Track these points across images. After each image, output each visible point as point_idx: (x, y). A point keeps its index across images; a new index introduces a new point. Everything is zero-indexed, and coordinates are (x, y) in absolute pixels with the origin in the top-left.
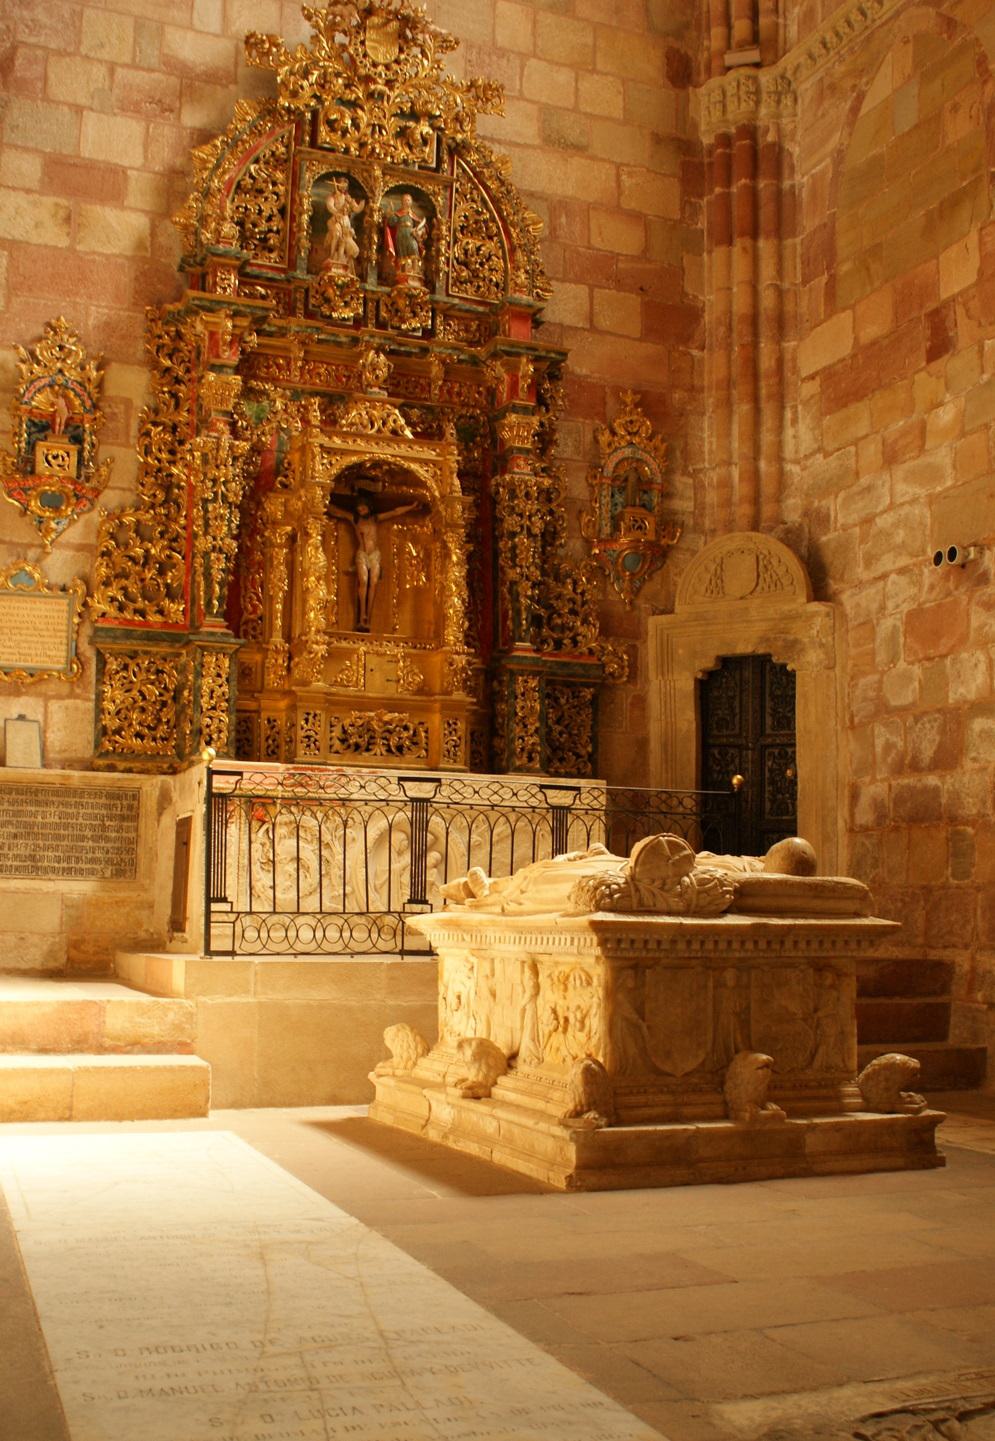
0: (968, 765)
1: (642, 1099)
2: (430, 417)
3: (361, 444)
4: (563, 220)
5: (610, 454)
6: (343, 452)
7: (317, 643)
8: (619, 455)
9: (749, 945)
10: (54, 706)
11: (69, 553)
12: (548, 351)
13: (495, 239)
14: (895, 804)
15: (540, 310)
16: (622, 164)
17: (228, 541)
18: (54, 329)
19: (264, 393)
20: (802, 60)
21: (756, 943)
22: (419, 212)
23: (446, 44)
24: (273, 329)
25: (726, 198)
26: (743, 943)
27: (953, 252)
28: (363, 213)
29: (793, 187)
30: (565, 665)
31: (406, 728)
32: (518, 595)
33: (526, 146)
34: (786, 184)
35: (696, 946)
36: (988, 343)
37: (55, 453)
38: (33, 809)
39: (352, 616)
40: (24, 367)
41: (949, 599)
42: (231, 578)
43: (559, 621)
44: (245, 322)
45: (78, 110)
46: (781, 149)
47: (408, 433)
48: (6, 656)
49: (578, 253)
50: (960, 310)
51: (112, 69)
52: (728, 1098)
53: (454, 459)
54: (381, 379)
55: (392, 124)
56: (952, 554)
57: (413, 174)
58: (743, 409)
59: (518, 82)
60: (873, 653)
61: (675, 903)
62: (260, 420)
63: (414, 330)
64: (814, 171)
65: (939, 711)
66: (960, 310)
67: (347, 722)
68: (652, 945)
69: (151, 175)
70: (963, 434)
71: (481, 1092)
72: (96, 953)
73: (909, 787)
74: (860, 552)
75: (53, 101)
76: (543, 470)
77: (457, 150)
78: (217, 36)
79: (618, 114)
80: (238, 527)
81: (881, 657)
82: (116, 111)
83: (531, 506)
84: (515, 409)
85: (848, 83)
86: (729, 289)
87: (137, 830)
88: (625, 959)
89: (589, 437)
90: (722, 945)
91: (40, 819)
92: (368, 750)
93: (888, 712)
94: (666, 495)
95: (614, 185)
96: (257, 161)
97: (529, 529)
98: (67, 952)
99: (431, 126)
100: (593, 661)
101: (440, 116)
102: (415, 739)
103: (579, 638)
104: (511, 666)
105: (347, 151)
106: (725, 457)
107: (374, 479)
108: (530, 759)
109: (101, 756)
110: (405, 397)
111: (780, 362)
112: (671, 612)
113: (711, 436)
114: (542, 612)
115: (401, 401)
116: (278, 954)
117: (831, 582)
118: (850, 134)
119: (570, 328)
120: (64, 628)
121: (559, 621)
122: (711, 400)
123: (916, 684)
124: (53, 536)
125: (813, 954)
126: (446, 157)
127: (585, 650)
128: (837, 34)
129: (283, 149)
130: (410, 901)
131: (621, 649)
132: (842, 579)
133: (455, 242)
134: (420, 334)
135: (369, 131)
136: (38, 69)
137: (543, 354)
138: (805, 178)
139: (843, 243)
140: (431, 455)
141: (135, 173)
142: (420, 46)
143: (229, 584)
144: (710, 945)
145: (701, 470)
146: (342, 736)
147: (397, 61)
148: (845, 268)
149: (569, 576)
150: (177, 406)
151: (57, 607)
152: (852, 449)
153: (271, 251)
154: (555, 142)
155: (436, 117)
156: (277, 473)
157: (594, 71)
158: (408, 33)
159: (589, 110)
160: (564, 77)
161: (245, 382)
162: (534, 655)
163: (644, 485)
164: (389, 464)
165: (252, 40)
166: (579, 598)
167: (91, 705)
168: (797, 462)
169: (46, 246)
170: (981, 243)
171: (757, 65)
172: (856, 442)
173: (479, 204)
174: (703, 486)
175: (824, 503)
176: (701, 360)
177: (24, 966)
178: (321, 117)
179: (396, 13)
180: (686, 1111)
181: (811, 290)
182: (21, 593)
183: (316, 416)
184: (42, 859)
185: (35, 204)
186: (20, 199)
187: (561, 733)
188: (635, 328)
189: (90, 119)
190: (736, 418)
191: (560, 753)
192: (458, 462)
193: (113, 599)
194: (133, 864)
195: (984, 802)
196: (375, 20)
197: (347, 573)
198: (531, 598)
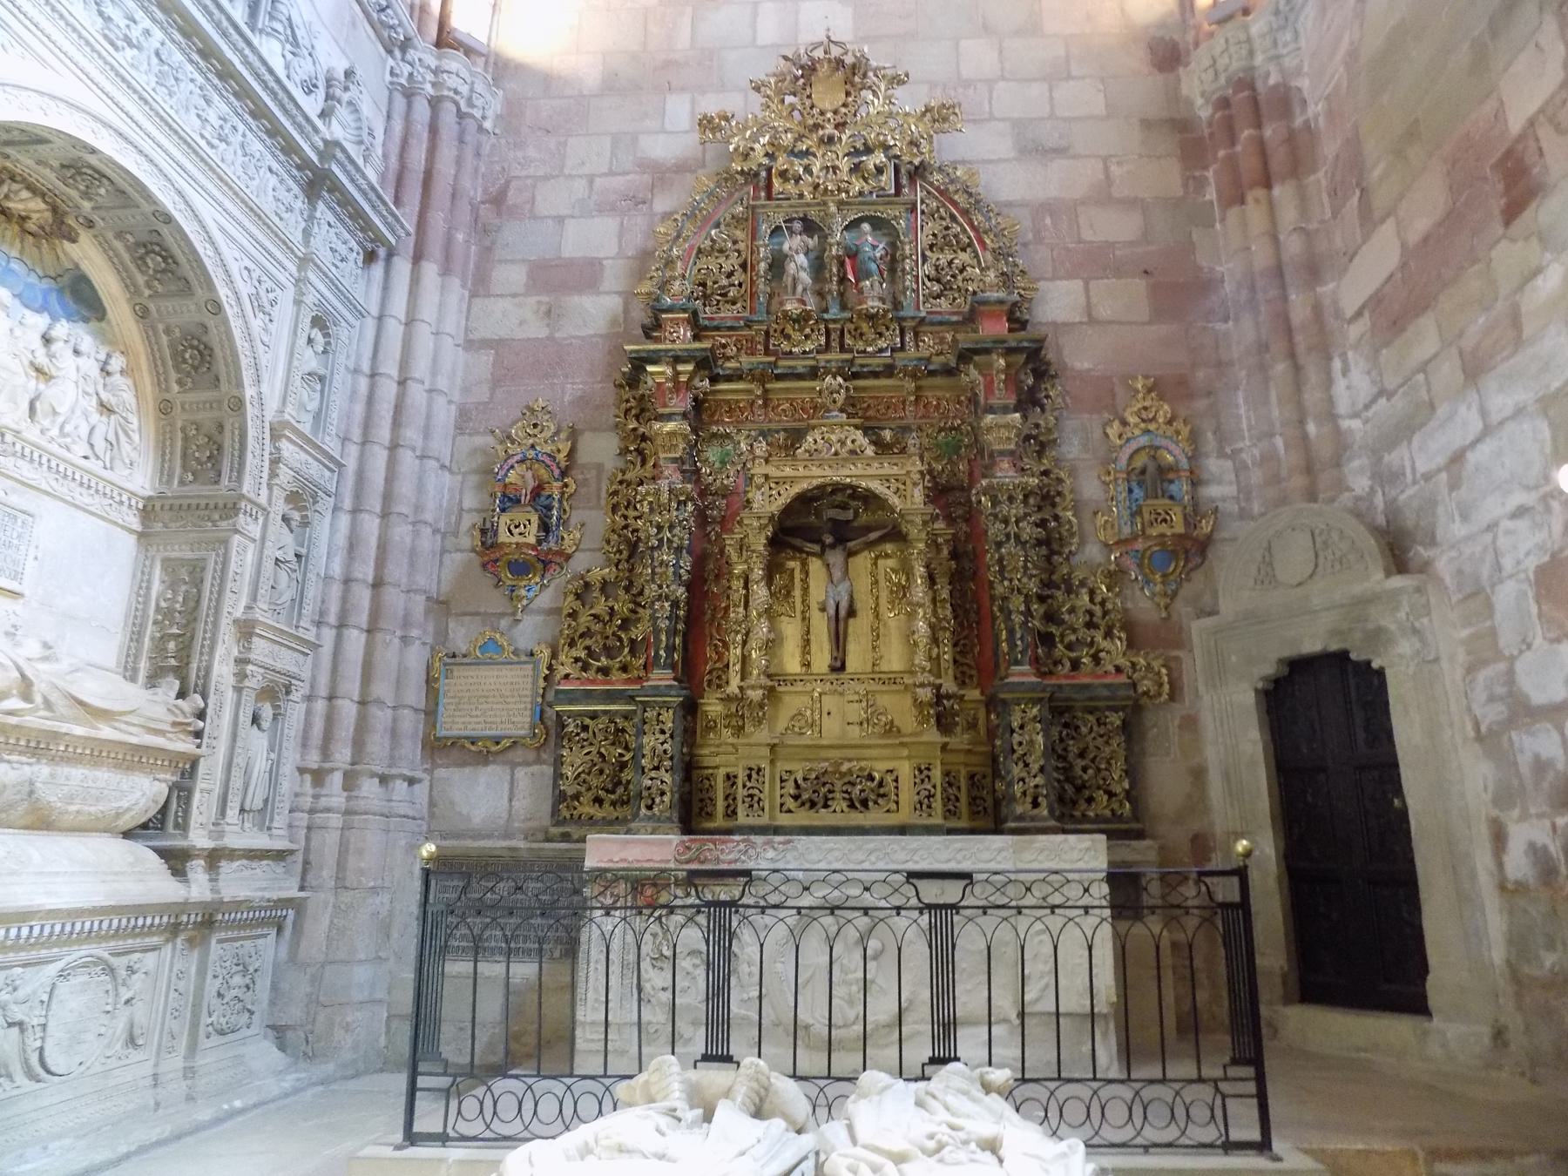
5: (1121, 447)
6: (792, 480)
8: (1134, 445)
10: (521, 773)
11: (539, 618)
13: (968, 250)
18: (532, 411)
19: (728, 436)
23: (897, 81)
25: (1231, 161)
31: (871, 778)
33: (1000, 161)
40: (499, 447)
45: (560, 220)
51: (591, 179)
54: (839, 404)
55: (845, 164)
60: (1493, 633)
63: (881, 350)
75: (541, 218)
77: (919, 172)
78: (686, 132)
82: (594, 213)
83: (1016, 510)
84: (991, 410)
89: (1098, 433)
94: (1196, 483)
95: (1102, 177)
96: (717, 225)
97: (1017, 537)
102: (882, 791)
104: (1002, 696)
105: (801, 196)
108: (1035, 804)
111: (1317, 310)
113: (1249, 410)
119: (1065, 324)
120: (529, 693)
122: (1243, 373)
124: (525, 602)
126: (904, 181)
127: (1111, 668)
131: (1156, 664)
132: (1432, 542)
140: (888, 469)
141: (610, 261)
142: (870, 88)
145: (1241, 450)
146: (796, 792)
150: (644, 463)
151: (522, 673)
152: (1421, 377)
153: (734, 303)
154: (1033, 150)
155: (891, 147)
157: (1069, 77)
159: (1067, 114)
163: (1164, 473)
166: (1097, 610)
172: (1423, 368)
173: (948, 220)
182: (492, 663)
186: (506, 304)
189: (571, 227)
193: (577, 660)
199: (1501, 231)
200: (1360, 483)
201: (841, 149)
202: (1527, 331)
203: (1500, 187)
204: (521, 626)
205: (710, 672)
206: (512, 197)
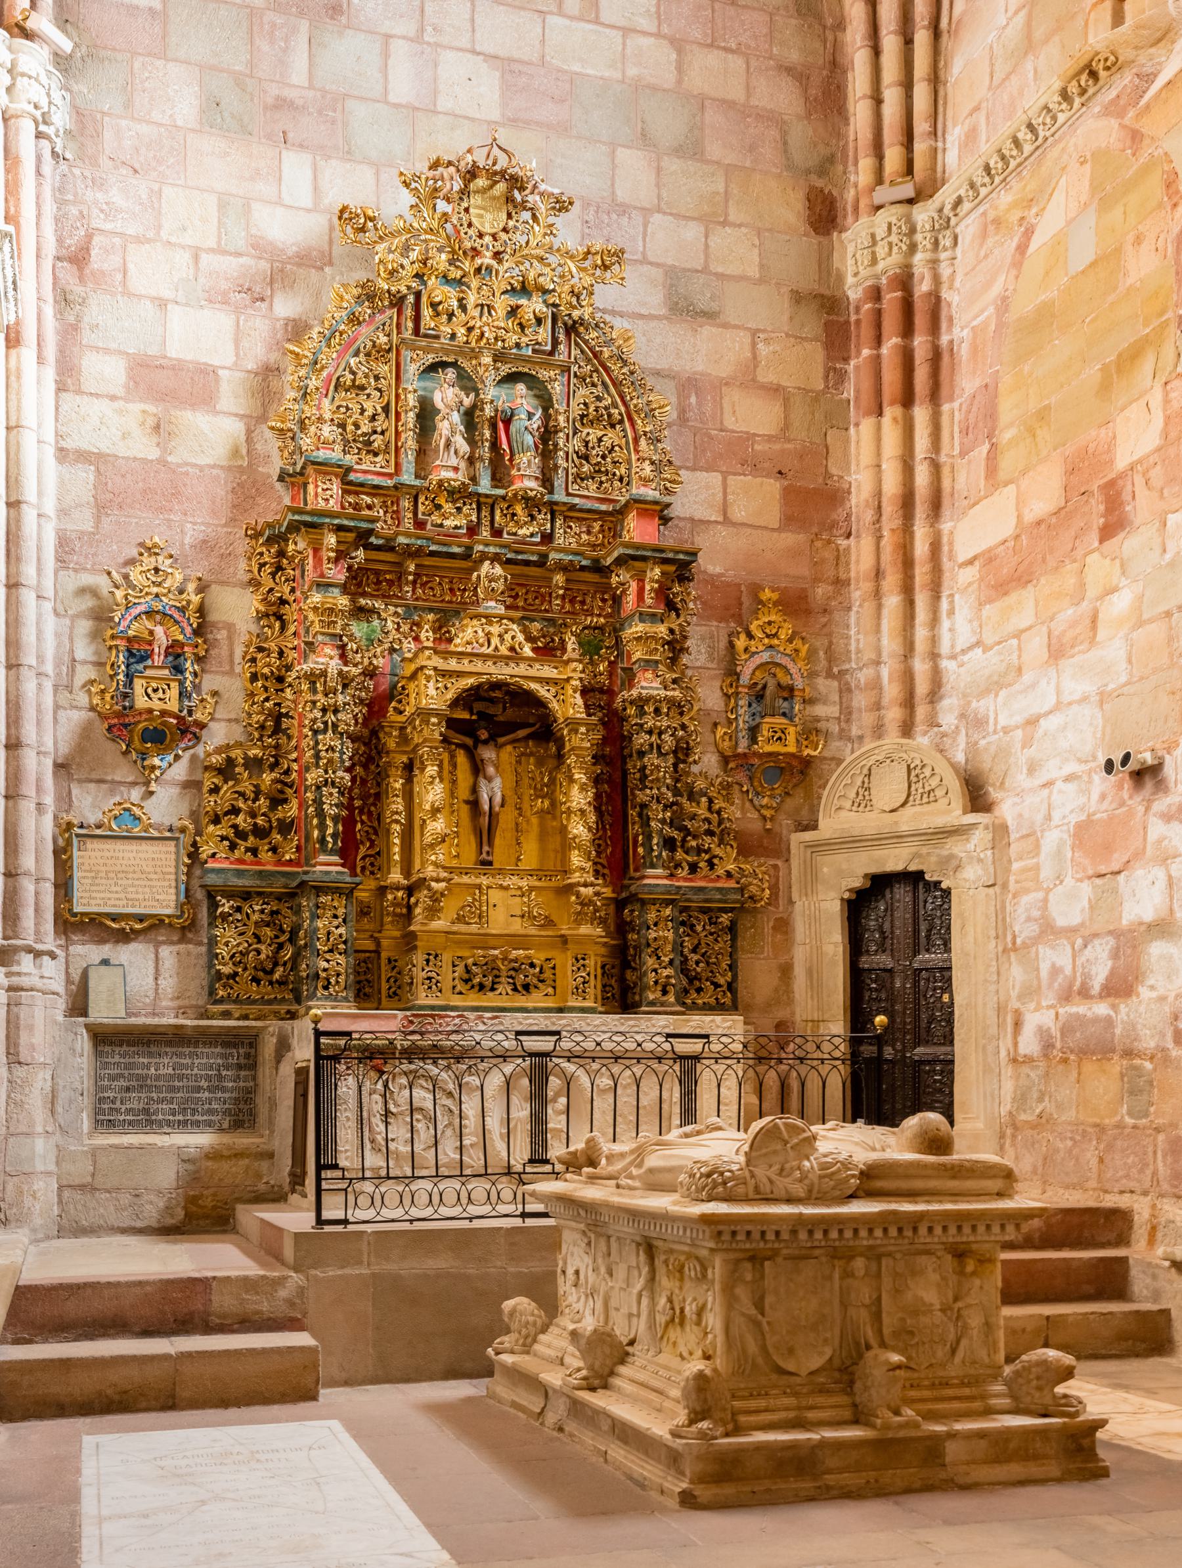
0: (1144, 992)
1: (762, 1403)
2: (552, 630)
3: (479, 666)
4: (693, 399)
7: (438, 880)
9: (878, 1233)
12: (678, 552)
14: (1062, 1034)
15: (668, 505)
16: (759, 330)
17: (340, 773)
19: (372, 611)
20: (962, 192)
21: (885, 1230)
22: (535, 402)
23: (561, 205)
24: (381, 542)
26: (871, 1231)
27: (1135, 411)
28: (474, 407)
29: (951, 342)
30: (701, 889)
32: (649, 819)
34: (944, 339)
35: (818, 1235)
36: (1172, 519)
37: (154, 685)
38: (146, 1061)
39: (474, 845)
41: (1125, 809)
42: (344, 813)
43: (694, 843)
44: (351, 536)
45: (162, 304)
46: (938, 299)
47: (527, 651)
48: (112, 902)
49: (711, 438)
50: (1139, 480)
52: (858, 1400)
53: (575, 672)
55: (502, 304)
56: (1126, 758)
57: (526, 360)
58: (893, 601)
59: (641, 243)
60: (1037, 868)
61: (799, 1190)
62: (371, 641)
64: (975, 323)
65: (1110, 933)
66: (1139, 480)
67: (470, 961)
68: (770, 1236)
69: (242, 375)
70: (1140, 624)
71: (596, 1382)
72: (214, 1207)
73: (1077, 1017)
74: (1021, 757)
76: (674, 681)
78: (308, 211)
79: (754, 272)
80: (351, 758)
81: (1046, 873)
85: (1014, 217)
86: (879, 466)
87: (254, 1078)
88: (741, 1250)
90: (848, 1234)
91: (153, 1070)
92: (493, 989)
93: (1053, 933)
96: (357, 354)
97: (659, 747)
98: (185, 1208)
99: (545, 302)
100: (732, 884)
101: (554, 290)
103: (716, 861)
105: (453, 336)
106: (873, 656)
107: (492, 701)
109: (216, 1002)
110: (524, 609)
112: (815, 827)
114: (676, 834)
115: (519, 614)
116: (393, 1221)
117: (991, 789)
118: (1017, 277)
121: (694, 843)
123: (1085, 903)
124: (158, 773)
125: (951, 1240)
126: (562, 337)
128: (1003, 158)
129: (385, 339)
130: (531, 1161)
133: (575, 434)
134: (538, 539)
135: (476, 313)
136: (115, 260)
137: (671, 555)
138: (966, 332)
139: (1007, 410)
141: (226, 372)
143: (344, 819)
144: (834, 1234)
147: (505, 230)
148: (1007, 435)
149: (705, 795)
150: (283, 628)
151: (164, 849)
152: (1015, 642)
153: (376, 454)
156: (391, 697)
158: (518, 196)
160: (692, 232)
161: (353, 601)
162: (666, 882)
164: (508, 684)
165: (346, 215)
167: (204, 949)
168: (953, 657)
169: (135, 459)
170: (1166, 401)
171: (911, 202)
172: (1018, 635)
174: (849, 690)
175: (982, 702)
176: (848, 549)
177: (139, 1224)
178: (424, 299)
179: (503, 173)
180: (811, 1415)
181: (970, 462)
183: (427, 635)
184: (156, 1112)
185: (120, 412)
187: (697, 963)
188: (773, 516)
190: (885, 612)
191: (697, 983)
192: (581, 679)
193: (223, 838)
194: (252, 1115)
195: (1163, 1035)
196: (481, 182)
197: (467, 802)
198: (663, 821)
199: (1096, 544)
200: (948, 719)
201: (500, 285)
202: (1101, 634)
203: (1102, 507)
204: (154, 797)
205: (363, 858)
206: (97, 260)
